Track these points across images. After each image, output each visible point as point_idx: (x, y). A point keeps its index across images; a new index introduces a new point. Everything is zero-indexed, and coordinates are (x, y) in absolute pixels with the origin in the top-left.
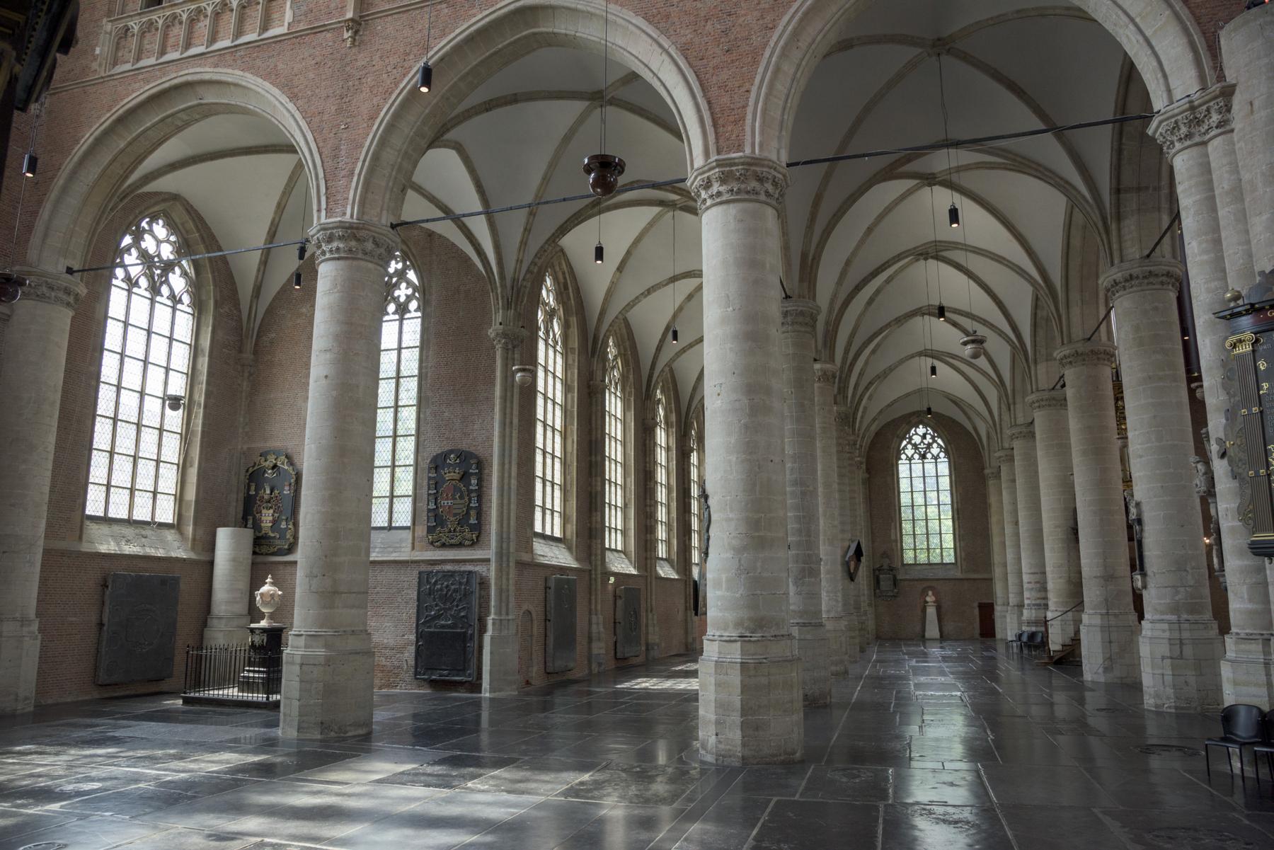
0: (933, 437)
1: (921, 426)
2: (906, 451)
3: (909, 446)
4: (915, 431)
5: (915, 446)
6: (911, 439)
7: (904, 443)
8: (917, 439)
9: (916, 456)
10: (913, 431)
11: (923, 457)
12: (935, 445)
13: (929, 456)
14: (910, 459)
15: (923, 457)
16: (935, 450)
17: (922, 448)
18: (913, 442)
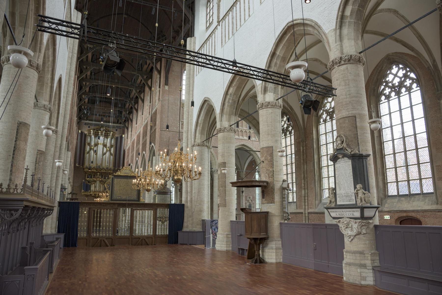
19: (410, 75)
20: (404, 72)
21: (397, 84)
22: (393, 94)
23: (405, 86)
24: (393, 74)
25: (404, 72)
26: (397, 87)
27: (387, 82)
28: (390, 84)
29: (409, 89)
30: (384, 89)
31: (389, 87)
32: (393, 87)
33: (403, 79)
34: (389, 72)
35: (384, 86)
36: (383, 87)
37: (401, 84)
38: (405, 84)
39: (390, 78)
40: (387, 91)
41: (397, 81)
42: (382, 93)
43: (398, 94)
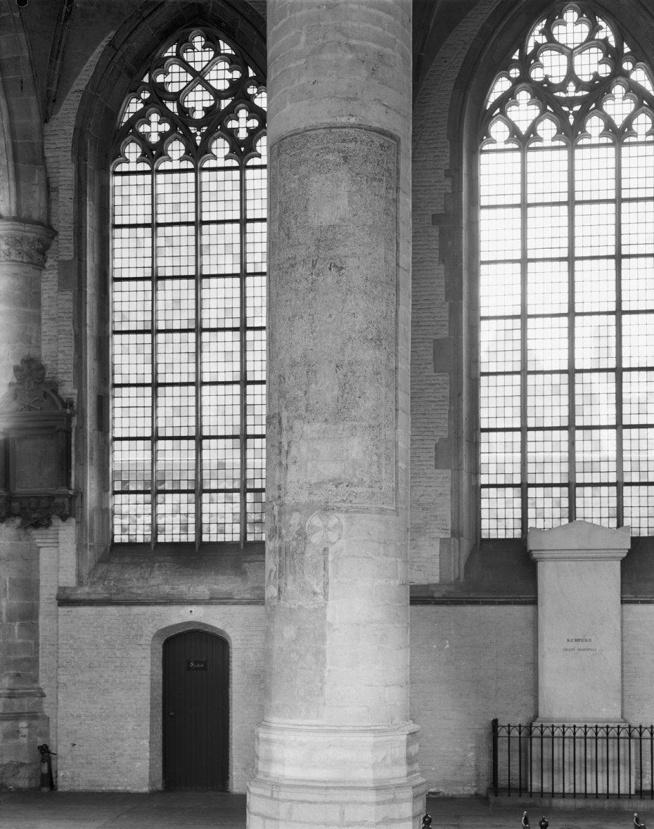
0: (613, 56)
1: (571, 16)
2: (513, 113)
3: (523, 96)
4: (547, 32)
5: (544, 94)
6: (526, 63)
7: (501, 86)
8: (551, 67)
9: (548, 129)
10: (536, 37)
11: (571, 134)
12: (618, 90)
13: (594, 125)
14: (523, 140)
15: (571, 134)
16: (618, 106)
17: (571, 102)
18: (537, 74)
19: (254, 96)
20: (237, 74)
21: (199, 115)
22: (176, 149)
23: (231, 135)
24: (186, 66)
25: (237, 74)
26: (200, 125)
27: (159, 95)
28: (172, 107)
29: (242, 150)
30: (142, 116)
31: (165, 116)
32: (181, 122)
33: (225, 103)
34: (172, 51)
35: (145, 102)
36: (135, 106)
37: (216, 120)
38: (232, 124)
39: (175, 79)
40: (154, 128)
41: (199, 101)
42: (131, 131)
43: (197, 153)
